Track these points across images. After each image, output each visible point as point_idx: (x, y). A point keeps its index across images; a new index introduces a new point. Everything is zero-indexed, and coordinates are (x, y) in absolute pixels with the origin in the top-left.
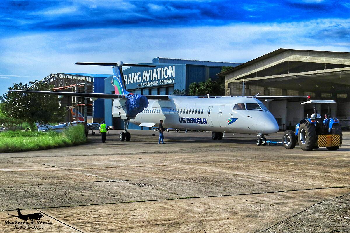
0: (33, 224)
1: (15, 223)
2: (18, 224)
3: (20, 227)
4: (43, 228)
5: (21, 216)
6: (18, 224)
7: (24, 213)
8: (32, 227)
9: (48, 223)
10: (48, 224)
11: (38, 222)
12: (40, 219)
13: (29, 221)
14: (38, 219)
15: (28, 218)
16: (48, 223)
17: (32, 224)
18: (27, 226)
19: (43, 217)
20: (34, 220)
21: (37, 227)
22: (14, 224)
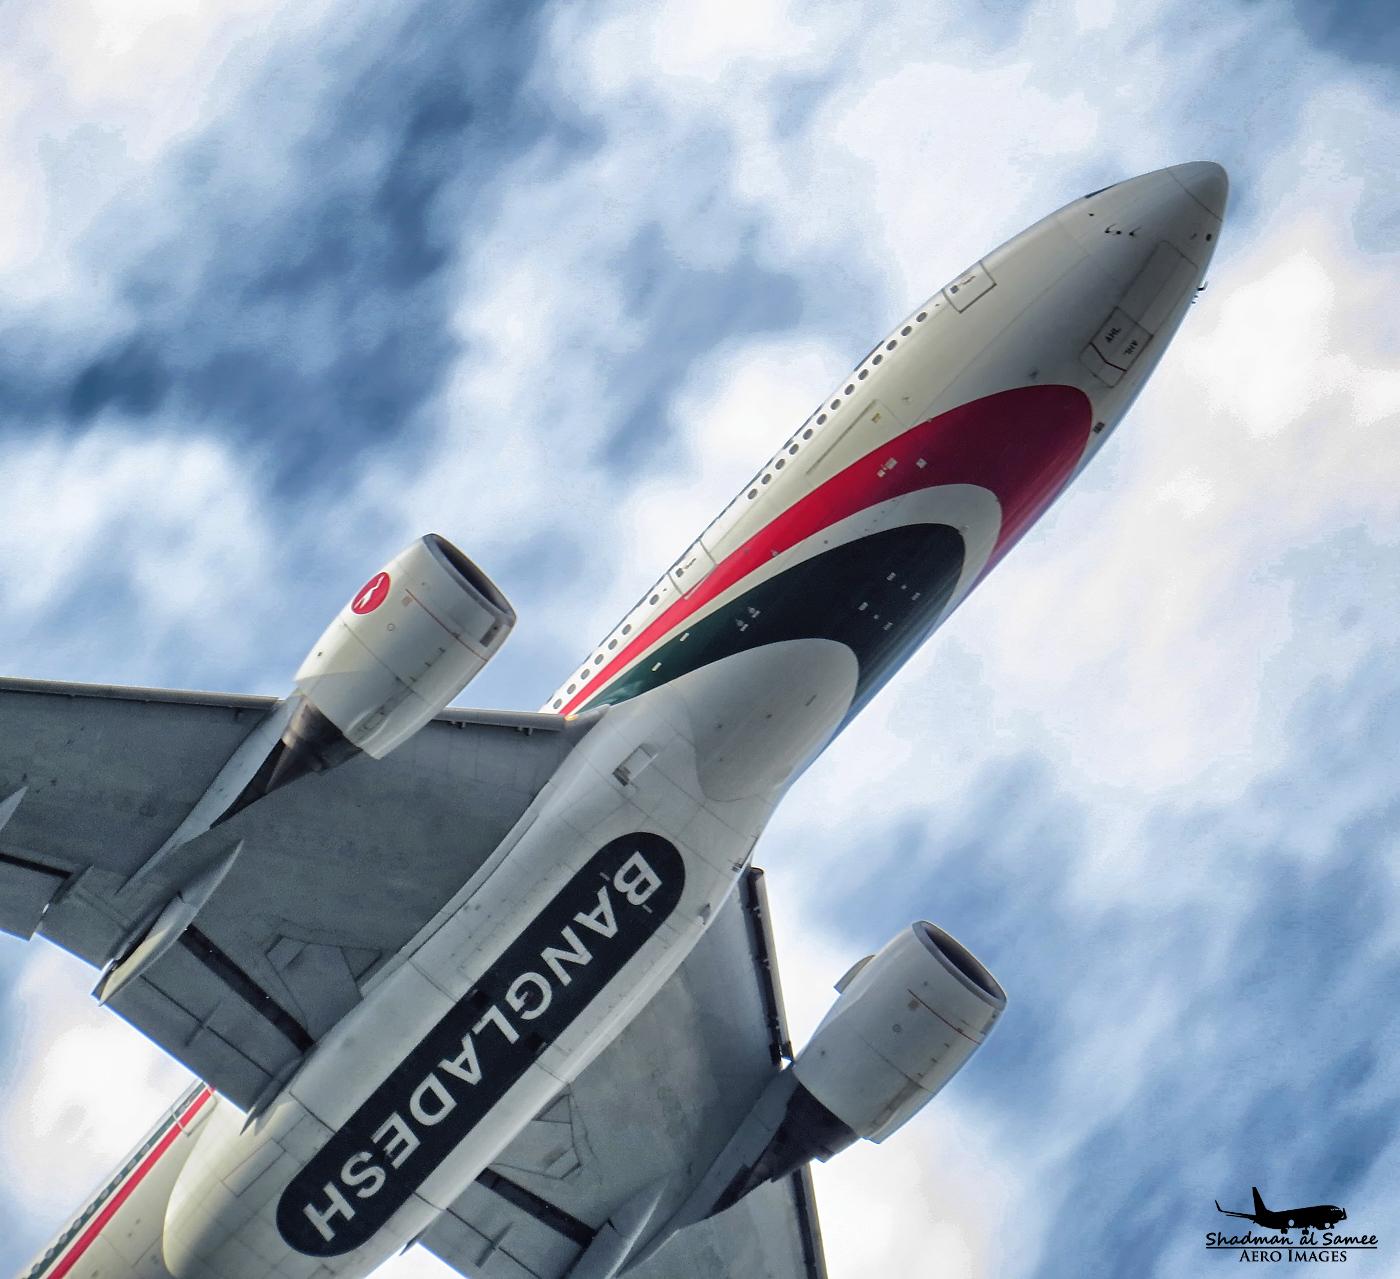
0: (1310, 1245)
1: (1242, 1242)
2: (1253, 1245)
3: (1259, 1255)
4: (1343, 1259)
5: (1264, 1217)
6: (1253, 1245)
7: (1275, 1204)
8: (1304, 1255)
9: (1363, 1242)
10: (1361, 1245)
11: (1327, 1237)
12: (1332, 1227)
13: (1294, 1234)
14: (1327, 1225)
15: (1291, 1223)
16: (1363, 1242)
17: (1305, 1245)
18: (1287, 1251)
19: (1345, 1218)
20: (1311, 1229)
21: (1324, 1256)
22: (1240, 1245)
